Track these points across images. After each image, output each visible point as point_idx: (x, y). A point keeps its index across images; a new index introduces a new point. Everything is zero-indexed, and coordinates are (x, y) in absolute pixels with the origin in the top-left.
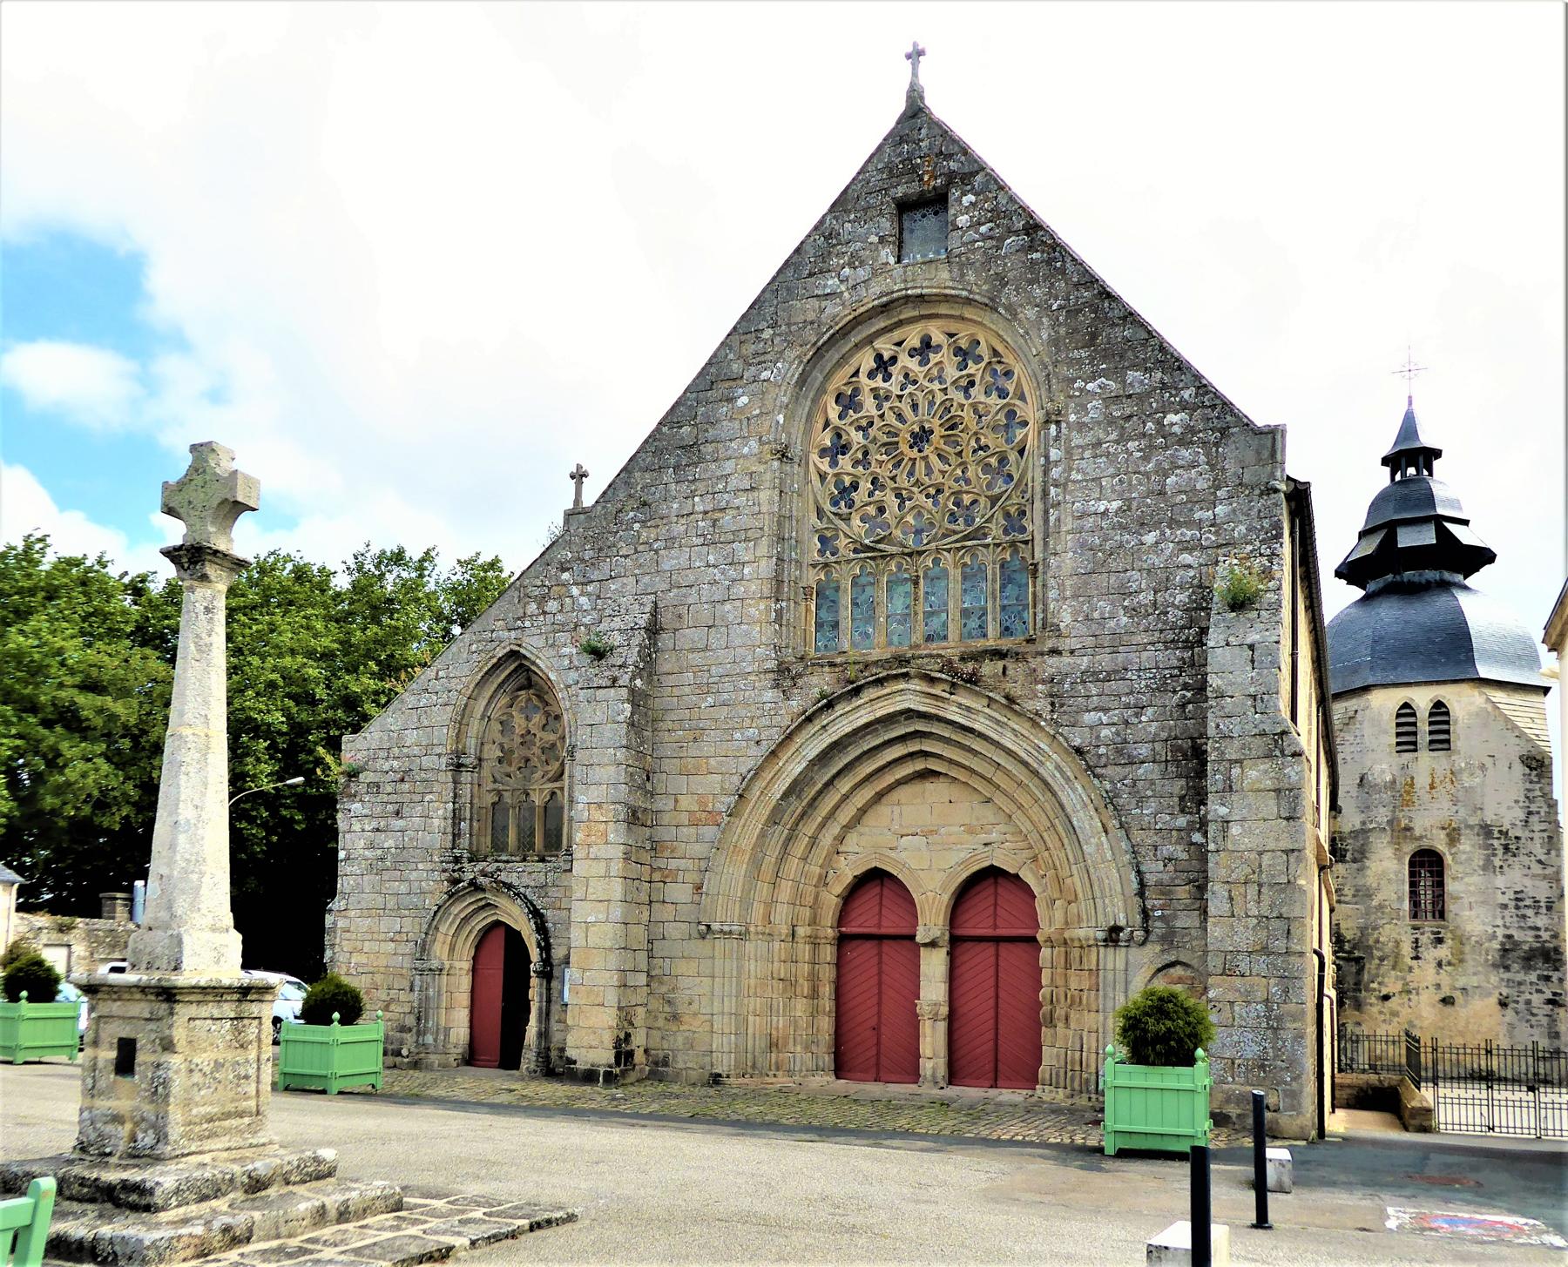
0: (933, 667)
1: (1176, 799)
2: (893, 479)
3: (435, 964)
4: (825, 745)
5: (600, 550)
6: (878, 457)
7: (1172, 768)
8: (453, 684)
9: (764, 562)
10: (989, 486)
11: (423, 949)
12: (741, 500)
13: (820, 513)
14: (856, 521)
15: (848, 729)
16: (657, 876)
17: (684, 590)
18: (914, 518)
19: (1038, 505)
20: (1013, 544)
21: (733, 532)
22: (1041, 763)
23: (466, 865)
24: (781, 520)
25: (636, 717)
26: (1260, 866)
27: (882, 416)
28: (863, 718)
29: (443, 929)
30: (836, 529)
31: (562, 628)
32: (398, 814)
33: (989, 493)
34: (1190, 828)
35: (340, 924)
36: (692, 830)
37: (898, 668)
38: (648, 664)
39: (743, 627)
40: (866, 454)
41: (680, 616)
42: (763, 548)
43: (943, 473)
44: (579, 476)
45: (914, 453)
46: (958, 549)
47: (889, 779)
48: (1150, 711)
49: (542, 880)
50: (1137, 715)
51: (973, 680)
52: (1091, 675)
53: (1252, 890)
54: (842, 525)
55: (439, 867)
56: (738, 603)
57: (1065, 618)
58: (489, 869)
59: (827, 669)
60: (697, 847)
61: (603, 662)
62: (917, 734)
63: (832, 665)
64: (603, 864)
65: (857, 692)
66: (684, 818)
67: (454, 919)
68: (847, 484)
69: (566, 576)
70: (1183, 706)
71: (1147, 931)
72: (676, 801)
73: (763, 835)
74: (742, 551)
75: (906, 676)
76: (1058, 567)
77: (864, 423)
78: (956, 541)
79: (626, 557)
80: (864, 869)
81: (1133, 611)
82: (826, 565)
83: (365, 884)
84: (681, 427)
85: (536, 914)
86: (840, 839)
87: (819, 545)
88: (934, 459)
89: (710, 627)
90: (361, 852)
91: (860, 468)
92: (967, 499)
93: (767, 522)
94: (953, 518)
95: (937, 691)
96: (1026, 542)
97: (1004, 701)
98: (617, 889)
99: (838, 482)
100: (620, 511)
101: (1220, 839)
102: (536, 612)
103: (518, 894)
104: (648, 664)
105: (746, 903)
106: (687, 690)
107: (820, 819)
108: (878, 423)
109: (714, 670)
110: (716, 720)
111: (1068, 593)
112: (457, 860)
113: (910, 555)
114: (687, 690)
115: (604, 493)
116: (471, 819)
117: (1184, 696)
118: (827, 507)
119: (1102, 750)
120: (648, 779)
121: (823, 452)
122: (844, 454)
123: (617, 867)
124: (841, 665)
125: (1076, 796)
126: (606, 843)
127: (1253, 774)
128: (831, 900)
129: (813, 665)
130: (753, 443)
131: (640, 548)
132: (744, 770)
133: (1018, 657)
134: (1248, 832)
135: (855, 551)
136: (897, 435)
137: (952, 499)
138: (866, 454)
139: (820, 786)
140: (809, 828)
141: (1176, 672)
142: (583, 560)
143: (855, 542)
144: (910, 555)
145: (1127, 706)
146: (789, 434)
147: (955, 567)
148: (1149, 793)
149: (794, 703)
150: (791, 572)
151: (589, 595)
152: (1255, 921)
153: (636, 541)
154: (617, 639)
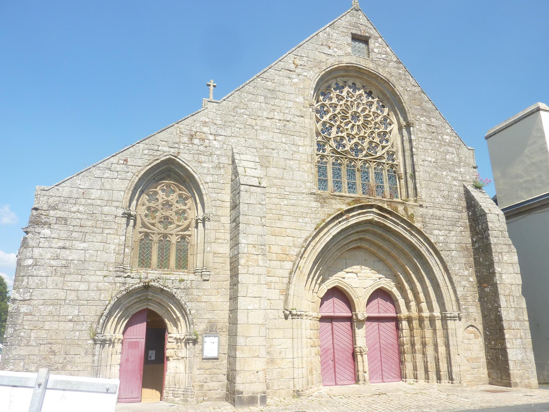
4: (339, 230)
5: (225, 122)
12: (296, 119)
31: (202, 153)
36: (278, 263)
48: (453, 232)
52: (433, 217)
56: (297, 162)
60: (281, 271)
72: (270, 248)
79: (240, 128)
90: (48, 261)
96: (397, 165)
106: (274, 195)
109: (287, 189)
110: (289, 212)
117: (461, 229)
126: (258, 266)
148: (456, 262)
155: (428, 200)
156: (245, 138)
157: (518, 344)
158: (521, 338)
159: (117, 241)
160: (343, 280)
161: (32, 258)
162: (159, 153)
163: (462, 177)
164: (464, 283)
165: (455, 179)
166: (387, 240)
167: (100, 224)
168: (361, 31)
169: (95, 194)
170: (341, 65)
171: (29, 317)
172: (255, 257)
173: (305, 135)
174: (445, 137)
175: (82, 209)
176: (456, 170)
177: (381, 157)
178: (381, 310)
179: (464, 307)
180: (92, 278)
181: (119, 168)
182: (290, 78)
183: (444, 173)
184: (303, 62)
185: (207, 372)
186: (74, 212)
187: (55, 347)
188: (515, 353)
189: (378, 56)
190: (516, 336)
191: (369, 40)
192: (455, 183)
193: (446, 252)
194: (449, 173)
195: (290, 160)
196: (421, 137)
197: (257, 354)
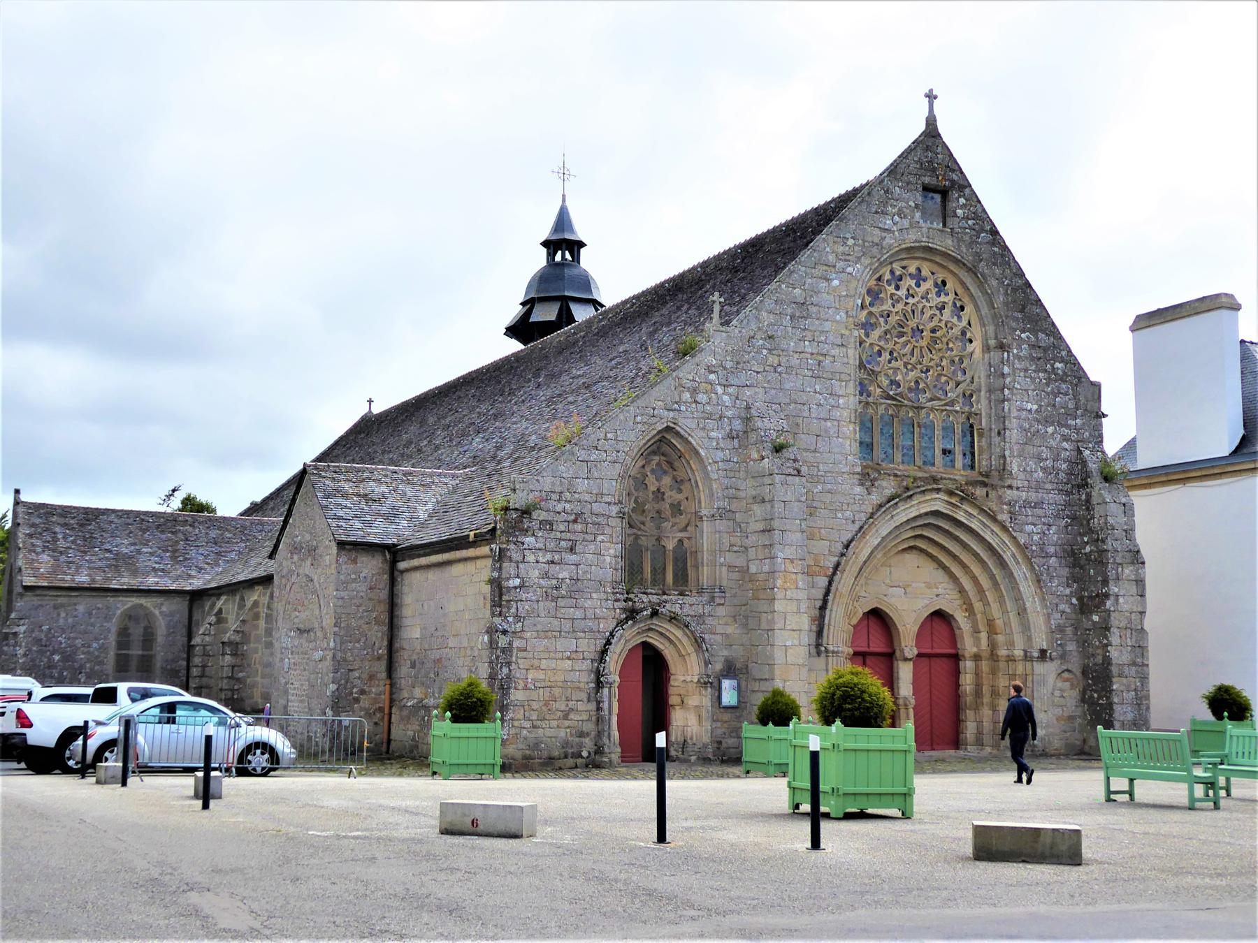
5: (738, 363)
7: (1063, 561)
8: (621, 446)
12: (835, 352)
17: (799, 406)
22: (1004, 552)
31: (710, 416)
32: (571, 550)
34: (1071, 595)
46: (943, 411)
48: (1054, 528)
50: (1049, 530)
52: (1027, 505)
56: (835, 423)
57: (1015, 469)
59: (892, 478)
63: (896, 475)
69: (712, 377)
70: (1066, 527)
75: (938, 490)
78: (942, 406)
79: (758, 373)
81: (1044, 469)
83: (541, 608)
84: (795, 288)
88: (909, 347)
89: (818, 436)
95: (953, 501)
96: (976, 414)
100: (753, 337)
102: (690, 400)
117: (1067, 522)
119: (1034, 548)
124: (900, 476)
125: (1021, 572)
126: (797, 588)
127: (1127, 571)
129: (885, 473)
134: (1126, 602)
135: (882, 398)
141: (1063, 507)
142: (725, 368)
145: (1044, 524)
151: (729, 394)
152: (1130, 648)
155: (1022, 476)
156: (765, 388)
157: (1131, 697)
159: (612, 551)
161: (518, 577)
163: (1077, 434)
164: (1062, 607)
165: (1065, 438)
166: (957, 539)
167: (591, 528)
168: (938, 178)
169: (582, 485)
171: (524, 654)
172: (794, 576)
173: (848, 378)
174: (1058, 365)
175: (567, 506)
177: (952, 403)
178: (935, 645)
179: (1059, 642)
180: (588, 603)
182: (827, 280)
183: (1050, 430)
184: (847, 248)
185: (725, 725)
186: (559, 513)
187: (557, 691)
189: (963, 223)
190: (1129, 686)
191: (950, 193)
192: (1065, 445)
193: (1041, 559)
194: (1058, 429)
195: (826, 420)
196: (1018, 369)
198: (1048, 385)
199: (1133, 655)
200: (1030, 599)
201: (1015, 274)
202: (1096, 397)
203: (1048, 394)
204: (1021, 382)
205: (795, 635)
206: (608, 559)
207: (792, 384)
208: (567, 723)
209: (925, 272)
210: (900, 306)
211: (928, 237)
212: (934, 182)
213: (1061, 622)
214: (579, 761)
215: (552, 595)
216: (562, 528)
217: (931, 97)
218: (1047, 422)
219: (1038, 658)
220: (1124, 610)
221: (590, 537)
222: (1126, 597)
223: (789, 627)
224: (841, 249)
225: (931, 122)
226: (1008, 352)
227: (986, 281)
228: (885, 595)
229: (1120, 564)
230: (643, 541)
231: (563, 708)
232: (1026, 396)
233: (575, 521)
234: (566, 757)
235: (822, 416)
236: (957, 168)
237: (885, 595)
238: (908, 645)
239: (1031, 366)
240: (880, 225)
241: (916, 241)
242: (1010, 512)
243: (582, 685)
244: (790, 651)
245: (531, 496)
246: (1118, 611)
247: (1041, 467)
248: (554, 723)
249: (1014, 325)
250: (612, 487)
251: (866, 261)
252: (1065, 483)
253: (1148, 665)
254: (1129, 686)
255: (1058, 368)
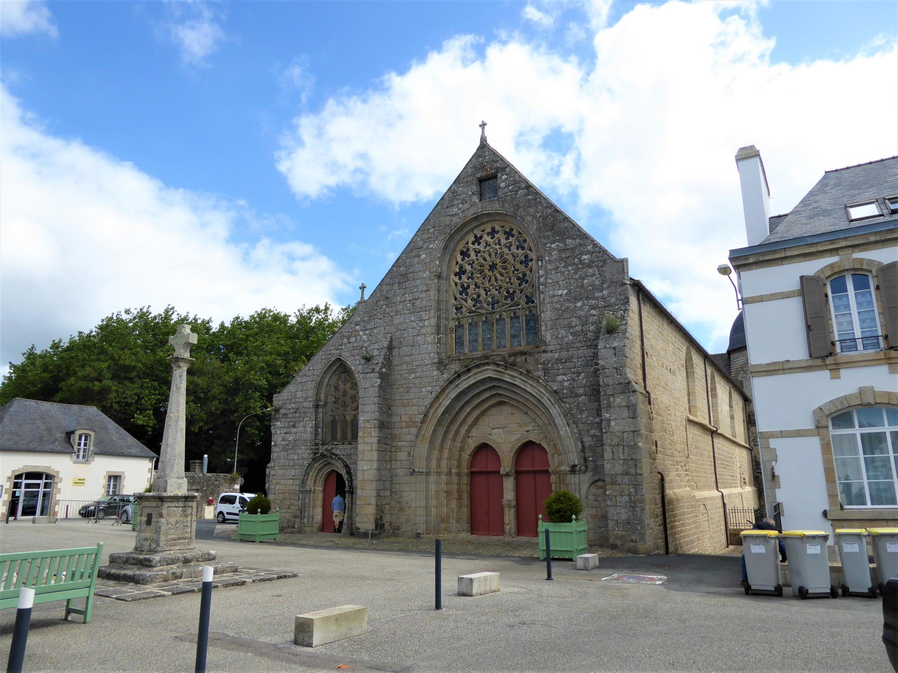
0: (497, 360)
1: (595, 411)
2: (483, 283)
3: (308, 488)
5: (371, 317)
6: (477, 275)
7: (592, 398)
8: (316, 372)
9: (432, 320)
10: (520, 285)
11: (304, 482)
13: (456, 299)
14: (469, 301)
15: (466, 386)
16: (394, 449)
17: (402, 332)
18: (492, 298)
19: (537, 293)
20: (529, 308)
21: (420, 308)
23: (320, 447)
24: (439, 302)
25: (383, 384)
26: (623, 438)
27: (477, 259)
28: (472, 381)
29: (311, 474)
30: (462, 304)
33: (519, 288)
35: (272, 473)
36: (407, 430)
37: (485, 361)
38: (388, 362)
39: (425, 346)
40: (472, 274)
41: (401, 342)
42: (432, 313)
43: (501, 280)
44: (363, 288)
45: (490, 273)
46: (509, 311)
47: (486, 406)
48: (583, 375)
49: (349, 452)
50: (578, 376)
51: (513, 364)
52: (559, 361)
53: (621, 448)
54: (465, 303)
55: (309, 448)
56: (423, 336)
57: (548, 338)
58: (329, 448)
59: (457, 361)
60: (409, 436)
61: (370, 362)
62: (494, 387)
63: (459, 360)
64: (370, 445)
65: (469, 370)
66: (404, 424)
67: (315, 470)
68: (465, 286)
69: (358, 327)
71: (586, 467)
72: (401, 418)
73: (435, 431)
74: (424, 315)
75: (488, 364)
76: (545, 317)
77: (471, 262)
78: (508, 307)
79: (380, 319)
80: (479, 443)
81: (573, 334)
82: (458, 319)
85: (346, 466)
86: (469, 431)
87: (455, 311)
91: (470, 280)
92: (511, 291)
93: (434, 304)
94: (506, 298)
96: (534, 307)
97: (525, 372)
98: (375, 455)
99: (462, 286)
100: (378, 301)
101: (607, 428)
103: (339, 459)
104: (388, 362)
105: (428, 458)
106: (404, 372)
107: (459, 423)
108: (476, 262)
110: (415, 384)
111: (549, 328)
112: (317, 445)
113: (490, 314)
114: (404, 372)
115: (372, 294)
116: (323, 428)
118: (458, 296)
119: (565, 391)
120: (389, 409)
121: (456, 274)
122: (464, 274)
123: (375, 446)
124: (463, 360)
125: (555, 411)
126: (371, 436)
128: (466, 456)
130: (428, 272)
131: (386, 315)
132: (426, 404)
133: (531, 354)
135: (469, 313)
136: (483, 266)
137: (505, 291)
138: (472, 274)
139: (457, 409)
140: (454, 428)
142: (364, 321)
143: (468, 309)
144: (490, 314)
145: (574, 373)
146: (441, 268)
147: (507, 318)
148: (584, 408)
149: (445, 376)
150: (443, 322)
153: (384, 313)
154: (376, 353)
157: (624, 501)
158: (629, 495)
159: (310, 425)
160: (490, 437)
162: (331, 356)
163: (604, 302)
164: (593, 432)
165: (592, 307)
169: (299, 394)
170: (467, 220)
172: (370, 429)
174: (584, 257)
175: (293, 405)
176: (596, 295)
179: (591, 459)
180: (300, 451)
181: (309, 373)
183: (579, 304)
188: (618, 511)
190: (622, 492)
192: (593, 312)
193: (572, 399)
194: (586, 302)
195: (417, 336)
197: (369, 502)
198: (576, 273)
199: (626, 467)
200: (564, 429)
201: (546, 208)
202: (620, 270)
203: (576, 279)
204: (553, 276)
205: (369, 463)
206: (309, 429)
207: (398, 321)
208: (290, 510)
209: (497, 228)
210: (506, 250)
211: (482, 208)
212: (484, 173)
213: (593, 443)
214: (294, 530)
215: (285, 449)
216: (291, 416)
217: (483, 125)
218: (576, 299)
219: (570, 471)
220: (616, 431)
221: (301, 419)
222: (617, 421)
223: (366, 459)
224: (426, 236)
225: (483, 140)
226: (541, 260)
227: (523, 220)
228: (490, 434)
229: (612, 395)
230: (337, 418)
231: (288, 503)
232: (558, 286)
233: (296, 412)
234: (289, 527)
235: (415, 334)
236: (499, 159)
237: (490, 434)
238: (507, 465)
239: (561, 264)
240: (450, 214)
241: (474, 214)
242: (544, 369)
243: (296, 492)
244: (366, 473)
245: (280, 403)
246: (609, 431)
247: (571, 333)
248: (285, 511)
249: (545, 241)
250: (311, 393)
251: (441, 238)
252: (594, 340)
253: (641, 475)
254: (622, 492)
255: (585, 259)
